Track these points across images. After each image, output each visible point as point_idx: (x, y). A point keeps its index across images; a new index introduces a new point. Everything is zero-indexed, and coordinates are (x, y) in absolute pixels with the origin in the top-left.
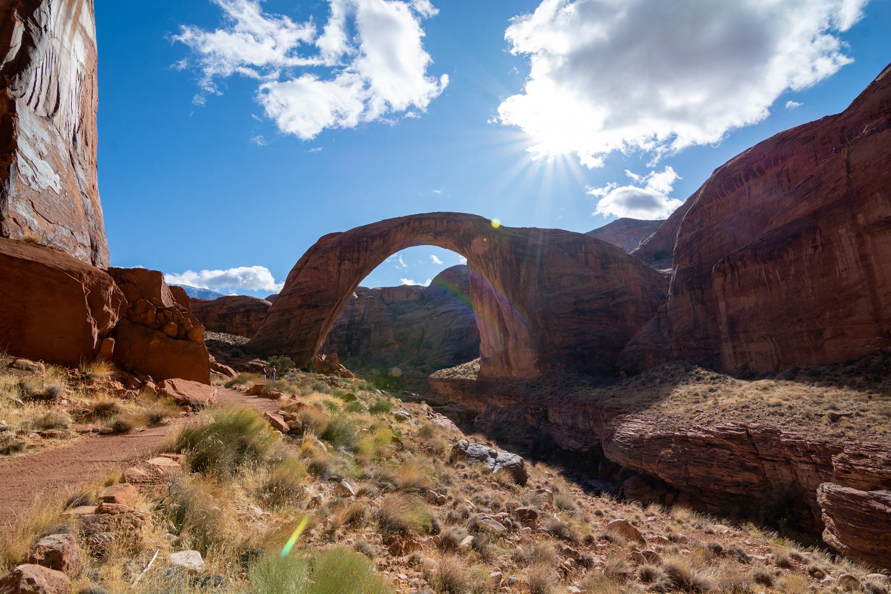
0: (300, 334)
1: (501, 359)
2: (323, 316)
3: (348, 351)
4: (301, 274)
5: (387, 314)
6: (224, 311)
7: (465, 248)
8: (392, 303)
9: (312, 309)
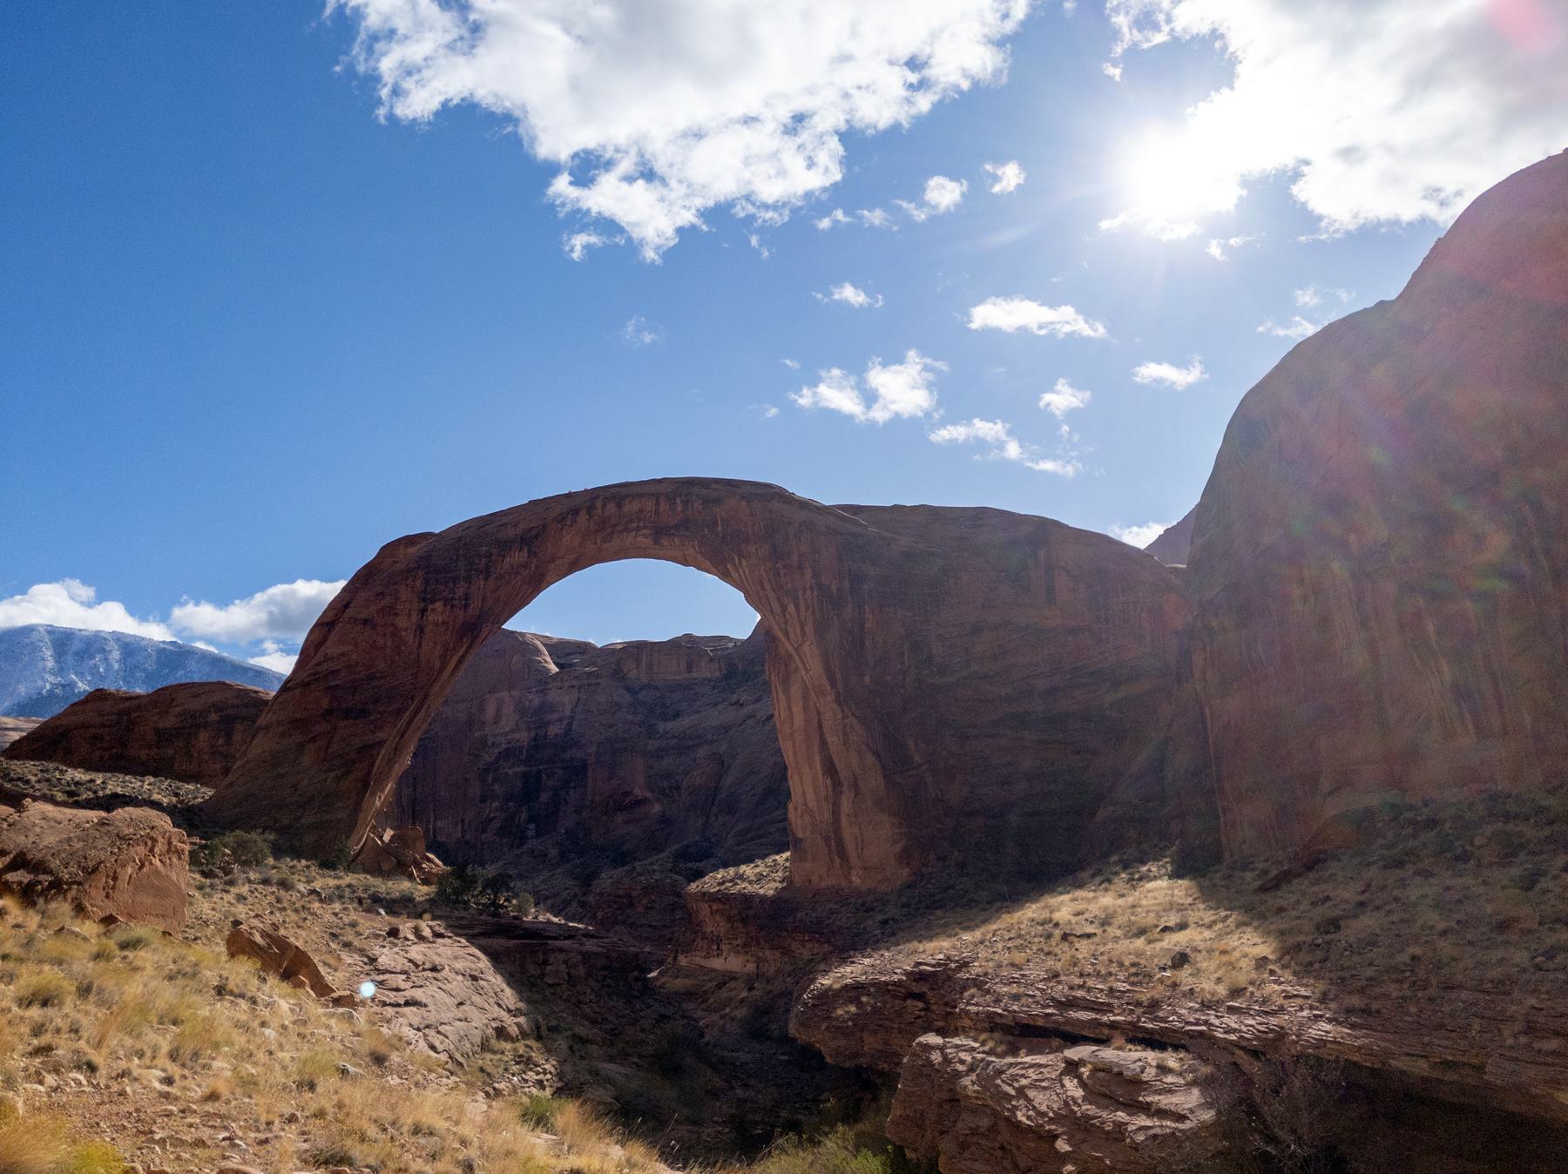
0: (325, 780)
1: (827, 839)
2: (380, 735)
3: (529, 820)
4: (333, 636)
5: (630, 717)
6: (168, 723)
7: (729, 566)
8: (644, 687)
9: (355, 719)
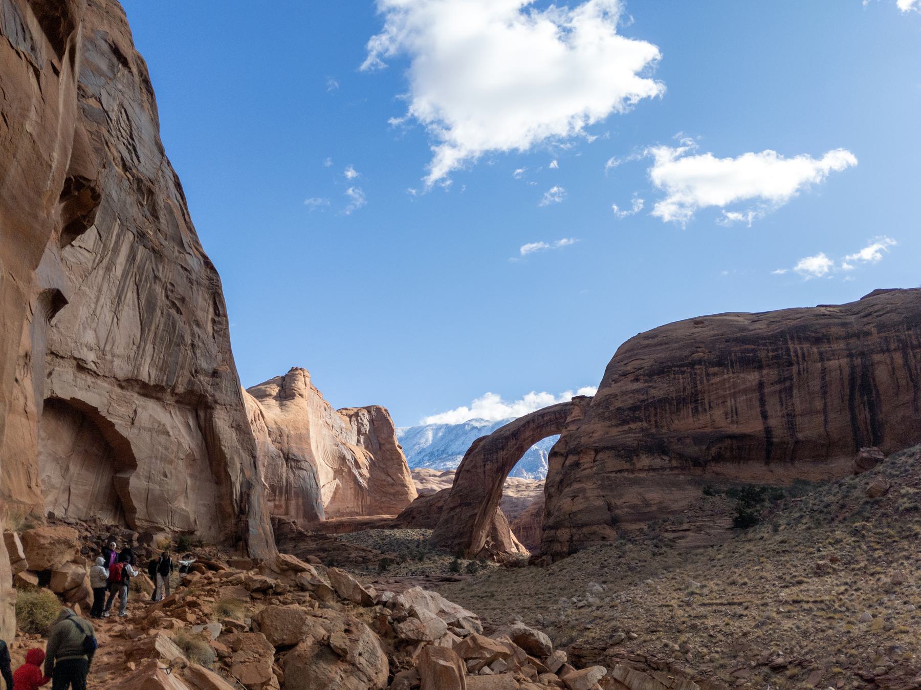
2: (476, 511)
